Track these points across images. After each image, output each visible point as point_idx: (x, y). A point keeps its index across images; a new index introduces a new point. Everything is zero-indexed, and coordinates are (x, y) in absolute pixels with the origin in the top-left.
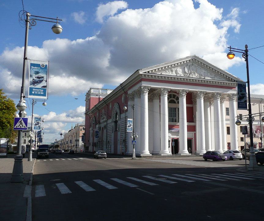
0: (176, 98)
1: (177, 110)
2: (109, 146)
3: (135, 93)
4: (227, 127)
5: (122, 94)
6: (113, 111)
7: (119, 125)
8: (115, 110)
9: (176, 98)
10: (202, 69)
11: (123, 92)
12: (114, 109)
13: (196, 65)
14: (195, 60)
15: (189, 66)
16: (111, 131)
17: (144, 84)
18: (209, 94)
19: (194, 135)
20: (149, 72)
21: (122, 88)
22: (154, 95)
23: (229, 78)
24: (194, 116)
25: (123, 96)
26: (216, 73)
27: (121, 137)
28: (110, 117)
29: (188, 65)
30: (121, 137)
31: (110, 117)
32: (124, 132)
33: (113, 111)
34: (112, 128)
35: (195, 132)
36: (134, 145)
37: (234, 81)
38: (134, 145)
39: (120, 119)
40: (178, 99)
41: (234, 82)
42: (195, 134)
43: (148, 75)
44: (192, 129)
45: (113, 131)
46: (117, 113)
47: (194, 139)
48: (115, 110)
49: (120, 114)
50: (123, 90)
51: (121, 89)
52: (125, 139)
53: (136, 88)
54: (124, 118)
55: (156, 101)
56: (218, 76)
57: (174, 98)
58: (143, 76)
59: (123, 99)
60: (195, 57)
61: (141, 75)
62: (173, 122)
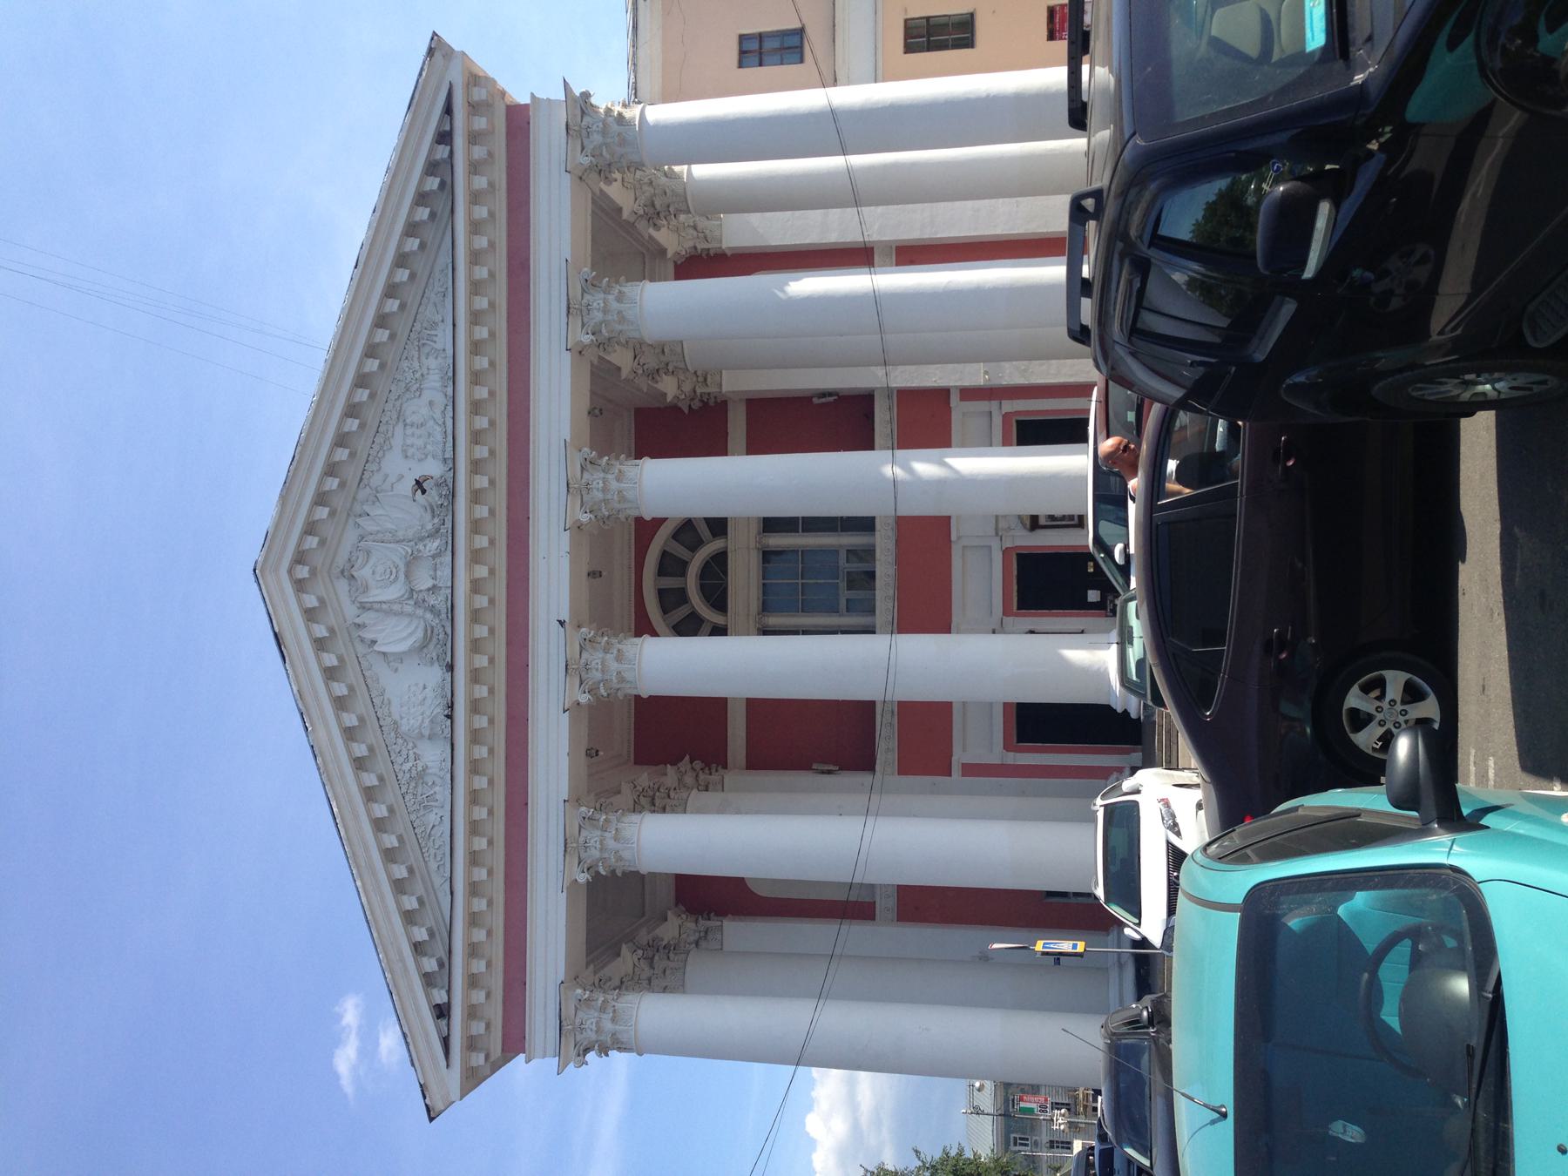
0: (680, 551)
1: (777, 541)
4: (909, 49)
9: (680, 551)
10: (376, 480)
13: (351, 536)
14: (300, 558)
20: (442, 1012)
37: (444, 137)
40: (688, 531)
41: (459, 141)
42: (969, 394)
43: (472, 1013)
44: (927, 419)
47: (1010, 406)
62: (871, 575)
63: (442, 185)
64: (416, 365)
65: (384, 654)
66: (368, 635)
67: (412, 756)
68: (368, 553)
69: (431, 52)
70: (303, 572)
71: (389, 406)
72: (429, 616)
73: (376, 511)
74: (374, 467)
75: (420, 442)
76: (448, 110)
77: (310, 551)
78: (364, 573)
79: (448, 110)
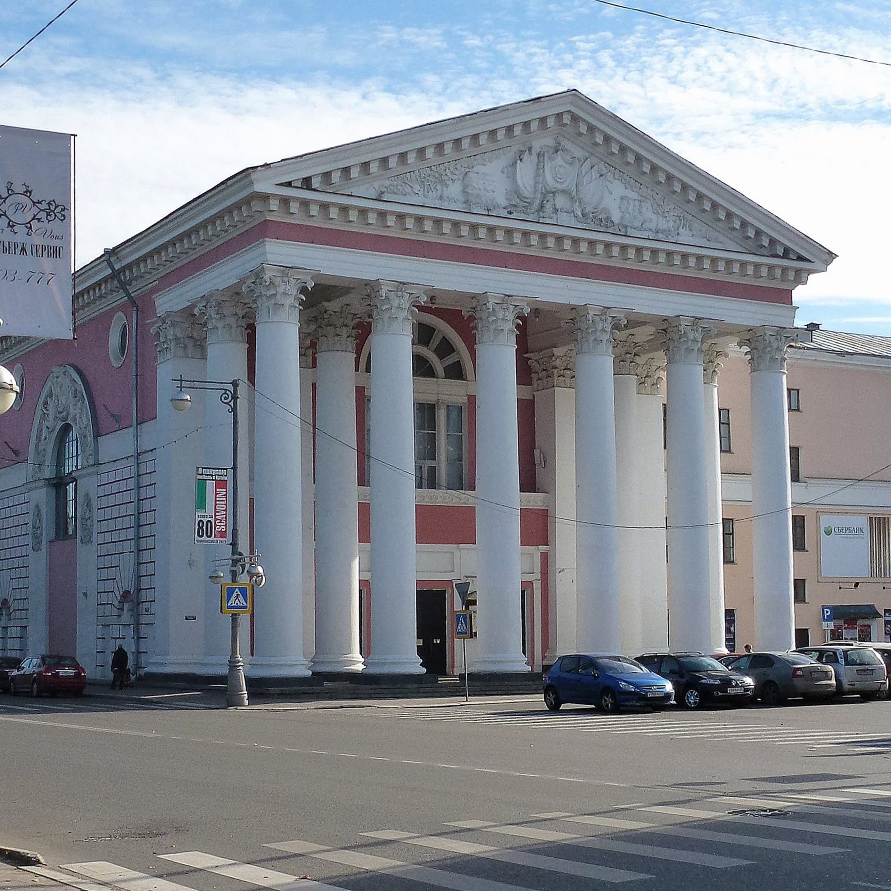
2: (14, 632)
3: (212, 312)
5: (109, 315)
6: (39, 413)
7: (89, 505)
8: (51, 411)
10: (610, 176)
11: (120, 297)
12: (46, 403)
13: (579, 153)
14: (575, 118)
15: (539, 155)
16: (29, 540)
17: (278, 252)
18: (643, 323)
19: (538, 568)
20: (307, 183)
21: (115, 275)
22: (335, 317)
23: (758, 233)
24: (537, 452)
25: (118, 321)
26: (689, 201)
27: (104, 574)
28: (16, 452)
29: (530, 149)
30: (104, 574)
31: (16, 452)
32: (130, 546)
33: (39, 413)
34: (29, 519)
35: (543, 548)
36: (234, 617)
38: (234, 617)
39: (97, 464)
43: (305, 204)
45: (37, 538)
46: (66, 428)
48: (51, 411)
49: (97, 435)
50: (123, 285)
51: (105, 280)
52: (139, 590)
53: (222, 276)
54: (132, 462)
55: (339, 365)
56: (697, 225)
57: (446, 337)
58: (274, 205)
59: (114, 339)
60: (572, 103)
61: (265, 197)
63: (762, 246)
64: (672, 213)
65: (514, 164)
66: (526, 157)
67: (455, 177)
68: (571, 164)
69: (830, 253)
70: (567, 119)
71: (649, 191)
72: (538, 202)
73: (594, 173)
74: (617, 177)
75: (630, 210)
76: (800, 258)
77: (579, 127)
78: (559, 159)
79: (800, 258)
